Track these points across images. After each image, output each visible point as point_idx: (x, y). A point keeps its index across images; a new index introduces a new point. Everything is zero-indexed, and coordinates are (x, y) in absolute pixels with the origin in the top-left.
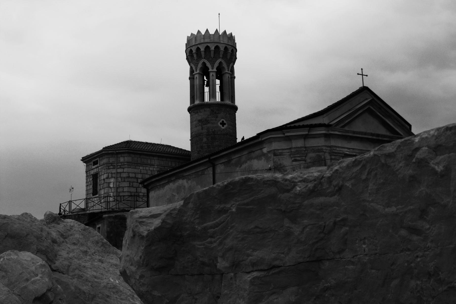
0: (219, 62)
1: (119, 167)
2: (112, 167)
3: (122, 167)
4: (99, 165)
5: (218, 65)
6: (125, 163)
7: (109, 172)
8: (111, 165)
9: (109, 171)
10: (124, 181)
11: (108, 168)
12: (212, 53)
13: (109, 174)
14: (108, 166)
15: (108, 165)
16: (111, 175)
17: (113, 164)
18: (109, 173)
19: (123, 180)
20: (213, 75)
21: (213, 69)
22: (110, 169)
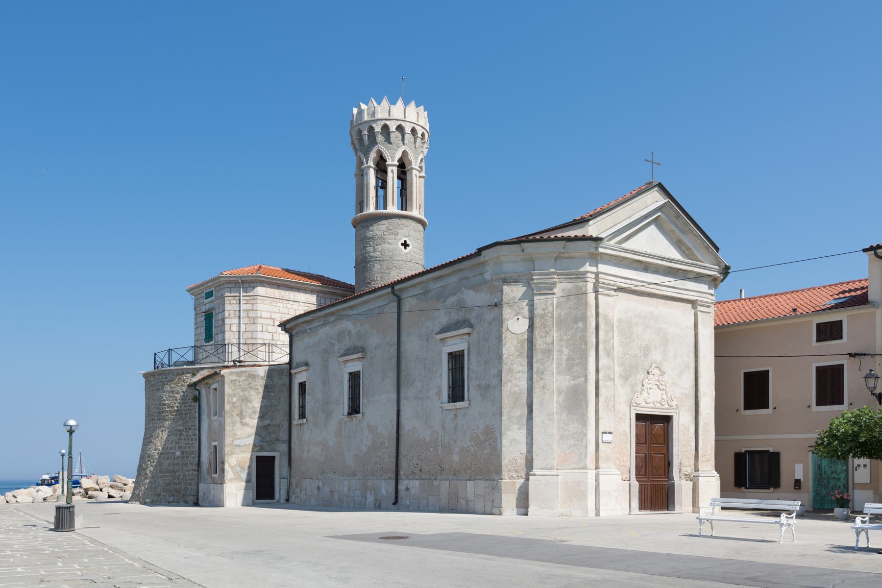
1: (246, 302)
2: (235, 302)
8: (233, 298)
10: (254, 323)
19: (252, 322)
22: (232, 304)
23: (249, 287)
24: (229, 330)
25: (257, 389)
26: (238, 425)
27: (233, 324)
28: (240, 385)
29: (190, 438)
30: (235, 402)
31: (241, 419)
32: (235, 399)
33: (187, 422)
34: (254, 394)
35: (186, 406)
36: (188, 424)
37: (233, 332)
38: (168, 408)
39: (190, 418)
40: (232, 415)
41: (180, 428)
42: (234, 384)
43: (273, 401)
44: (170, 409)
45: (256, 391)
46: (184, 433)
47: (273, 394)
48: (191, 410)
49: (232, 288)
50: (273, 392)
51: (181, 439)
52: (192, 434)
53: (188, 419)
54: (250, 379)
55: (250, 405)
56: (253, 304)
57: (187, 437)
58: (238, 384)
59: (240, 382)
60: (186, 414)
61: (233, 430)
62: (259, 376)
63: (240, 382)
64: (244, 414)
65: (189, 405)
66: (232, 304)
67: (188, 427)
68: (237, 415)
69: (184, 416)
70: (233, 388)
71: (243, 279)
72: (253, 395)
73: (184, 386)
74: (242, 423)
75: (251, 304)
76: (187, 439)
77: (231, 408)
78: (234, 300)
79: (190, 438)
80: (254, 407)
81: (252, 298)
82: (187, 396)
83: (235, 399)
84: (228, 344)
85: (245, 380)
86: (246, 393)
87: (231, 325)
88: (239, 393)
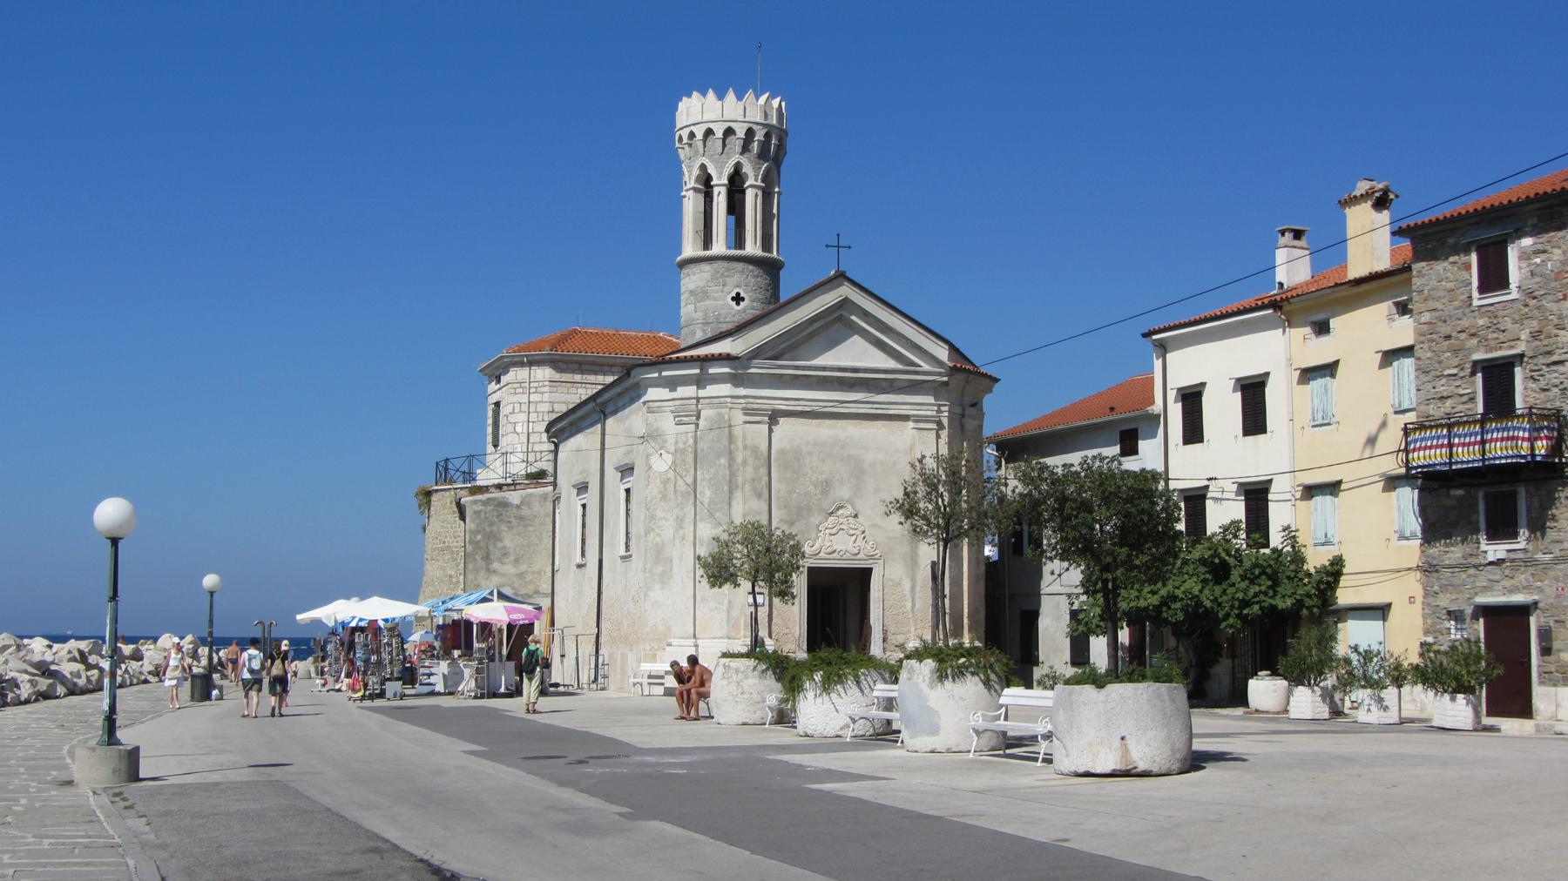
2: (521, 390)
3: (539, 390)
8: (519, 385)
19: (540, 419)
24: (513, 430)
25: (510, 522)
26: (482, 573)
28: (486, 518)
30: (479, 542)
31: (487, 564)
32: (479, 537)
34: (506, 529)
37: (518, 434)
40: (475, 560)
42: (479, 517)
43: (532, 539)
45: (509, 525)
47: (531, 529)
50: (531, 526)
54: (500, 509)
55: (500, 545)
56: (542, 393)
58: (483, 516)
59: (486, 513)
61: (476, 579)
62: (513, 504)
63: (486, 513)
64: (491, 557)
68: (482, 559)
70: (477, 522)
71: (530, 358)
72: (504, 531)
74: (488, 570)
77: (474, 550)
78: (521, 387)
80: (505, 547)
81: (541, 384)
83: (479, 537)
84: (507, 453)
85: (493, 510)
86: (495, 528)
87: (515, 423)
88: (484, 530)
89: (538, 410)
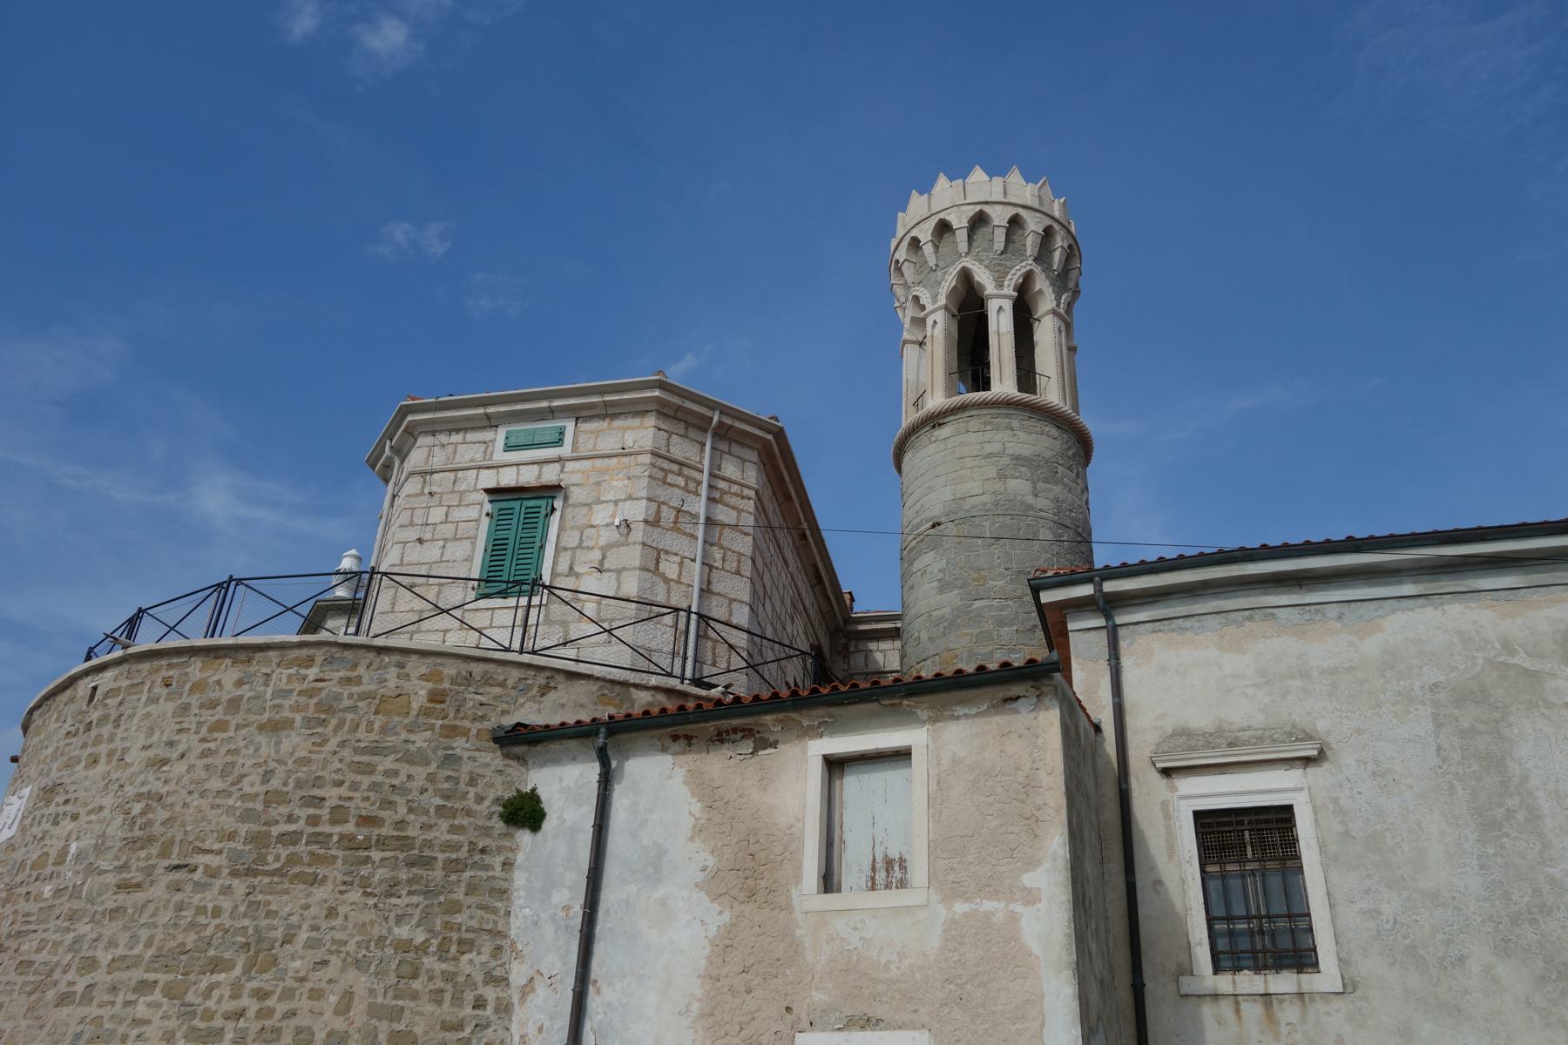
0: (1024, 270)
4: (575, 447)
5: (1021, 281)
6: (746, 492)
7: (662, 500)
8: (675, 467)
9: (663, 493)
10: (738, 573)
11: (660, 475)
12: (1000, 237)
13: (664, 508)
14: (662, 469)
15: (660, 462)
16: (672, 518)
17: (686, 471)
18: (663, 503)
20: (1001, 308)
21: (1000, 286)
22: (670, 485)
23: (729, 453)
24: (652, 567)
27: (667, 552)
29: (469, 997)
33: (454, 908)
35: (454, 829)
36: (459, 918)
37: (667, 580)
38: (334, 822)
39: (471, 890)
41: (402, 932)
44: (350, 827)
46: (429, 962)
48: (483, 851)
49: (674, 436)
51: (414, 996)
52: (479, 978)
53: (459, 895)
57: (449, 987)
60: (454, 866)
65: (477, 828)
66: (670, 485)
67: (455, 936)
69: (437, 874)
73: (465, 733)
75: (733, 508)
76: (448, 996)
79: (469, 997)
81: (735, 488)
82: (472, 782)
89: (725, 543)
